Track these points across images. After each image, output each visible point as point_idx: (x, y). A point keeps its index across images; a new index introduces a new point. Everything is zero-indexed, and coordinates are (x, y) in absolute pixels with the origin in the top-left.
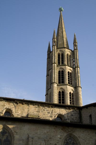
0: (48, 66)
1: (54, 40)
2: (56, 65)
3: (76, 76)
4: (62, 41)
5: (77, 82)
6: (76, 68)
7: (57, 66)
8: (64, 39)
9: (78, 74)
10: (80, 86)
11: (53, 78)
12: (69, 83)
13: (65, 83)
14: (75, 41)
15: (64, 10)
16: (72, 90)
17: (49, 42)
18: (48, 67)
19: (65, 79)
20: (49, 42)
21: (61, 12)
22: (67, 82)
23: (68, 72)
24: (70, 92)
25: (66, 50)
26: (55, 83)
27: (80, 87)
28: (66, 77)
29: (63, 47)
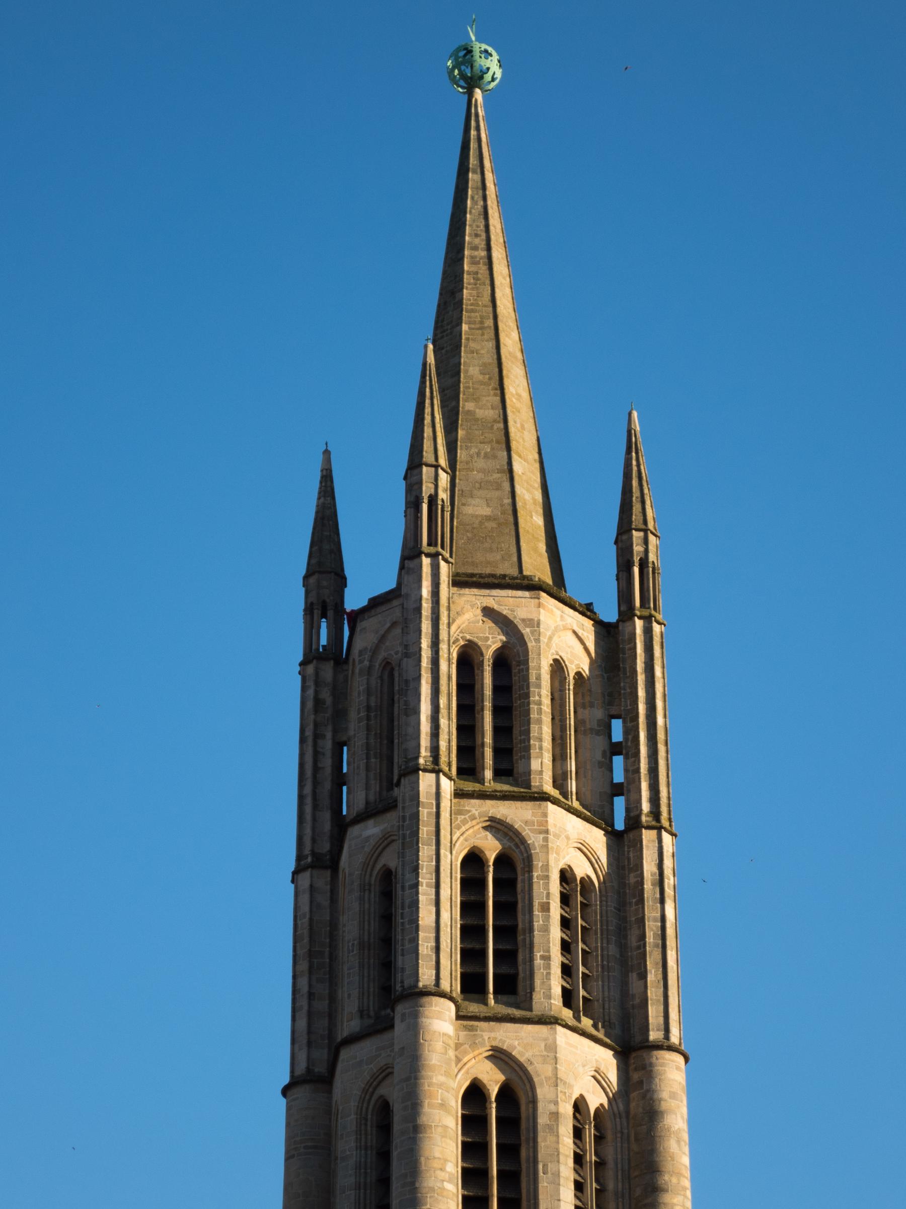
0: (316, 754)
1: (427, 489)
2: (444, 782)
3: (641, 921)
4: (498, 487)
5: (654, 993)
6: (648, 837)
7: (459, 794)
8: (517, 467)
9: (662, 901)
10: (674, 1039)
11: (415, 940)
12: (568, 997)
13: (538, 998)
14: (636, 508)
15: (503, 74)
16: (598, 1078)
17: (327, 453)
18: (316, 769)
19: (531, 960)
20: (327, 453)
21: (470, 94)
22: (556, 985)
23: (566, 876)
24: (575, 1095)
25: (543, 616)
26: (443, 995)
27: (672, 1048)
28: (546, 929)
29: (508, 569)
